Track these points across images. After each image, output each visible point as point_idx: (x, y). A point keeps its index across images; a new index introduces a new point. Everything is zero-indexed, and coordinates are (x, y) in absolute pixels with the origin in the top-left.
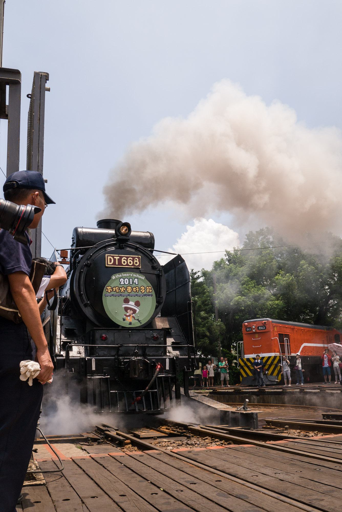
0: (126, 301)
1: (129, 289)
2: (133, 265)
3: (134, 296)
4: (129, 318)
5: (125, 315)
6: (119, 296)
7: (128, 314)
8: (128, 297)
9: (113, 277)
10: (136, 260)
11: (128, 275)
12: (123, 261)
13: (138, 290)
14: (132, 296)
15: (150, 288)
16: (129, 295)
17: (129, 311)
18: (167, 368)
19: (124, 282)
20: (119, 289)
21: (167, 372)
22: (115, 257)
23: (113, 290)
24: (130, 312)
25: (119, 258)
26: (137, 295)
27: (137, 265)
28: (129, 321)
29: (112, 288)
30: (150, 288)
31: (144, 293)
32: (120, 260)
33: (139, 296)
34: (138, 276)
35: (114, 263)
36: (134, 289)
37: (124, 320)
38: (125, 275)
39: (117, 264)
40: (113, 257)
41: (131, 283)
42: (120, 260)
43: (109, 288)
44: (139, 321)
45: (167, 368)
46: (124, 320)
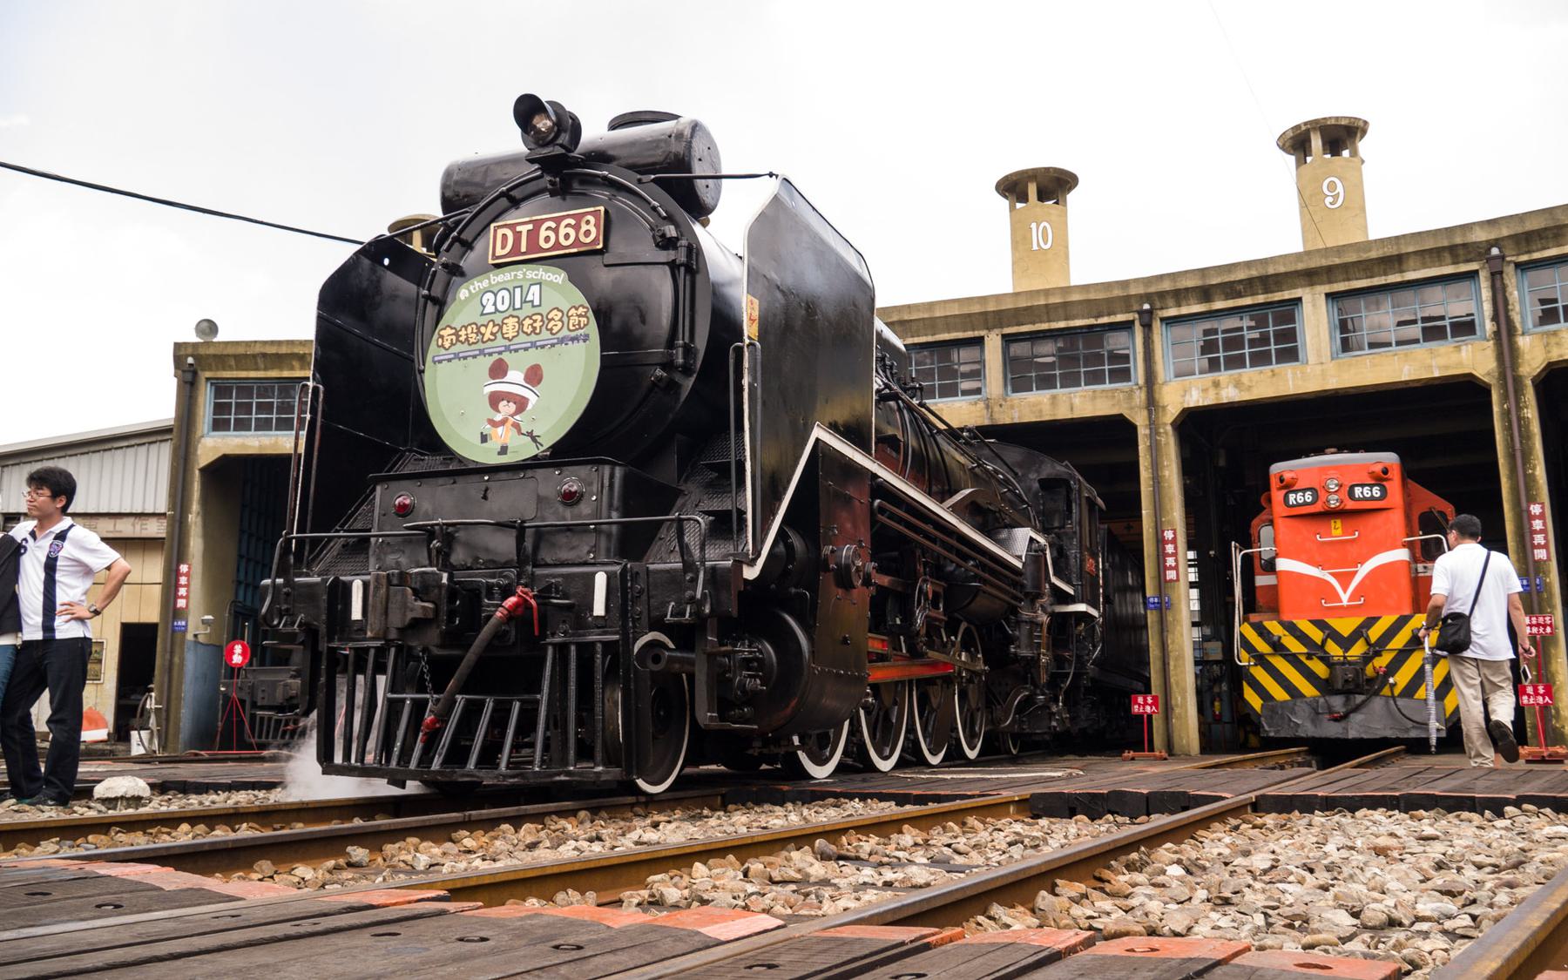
0: (498, 370)
1: (510, 327)
2: (577, 242)
3: (526, 349)
4: (500, 430)
6: (474, 357)
7: (498, 418)
8: (506, 356)
10: (588, 222)
12: (543, 233)
13: (538, 325)
15: (581, 310)
16: (507, 349)
18: (599, 609)
20: (478, 332)
21: (601, 624)
22: (519, 228)
23: (458, 336)
24: (507, 408)
25: (530, 227)
26: (534, 345)
27: (588, 240)
30: (581, 310)
31: (560, 335)
32: (533, 235)
33: (543, 347)
35: (516, 249)
37: (484, 438)
39: (523, 249)
40: (512, 227)
41: (518, 305)
42: (533, 235)
43: (449, 331)
44: (534, 439)
45: (599, 609)
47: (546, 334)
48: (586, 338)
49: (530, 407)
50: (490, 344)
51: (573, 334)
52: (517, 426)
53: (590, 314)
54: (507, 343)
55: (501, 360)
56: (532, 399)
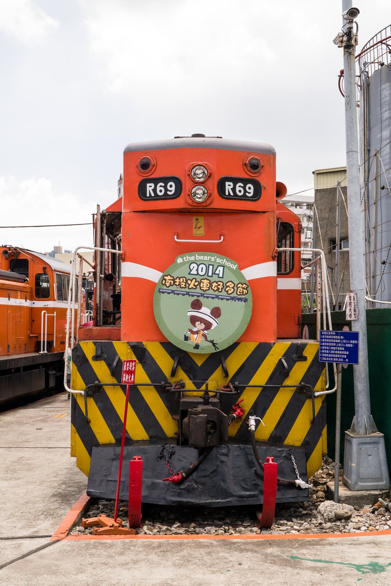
0: (197, 305)
1: (205, 284)
3: (213, 298)
4: (195, 336)
5: (191, 331)
7: (195, 330)
8: (201, 299)
9: (179, 260)
11: (206, 258)
13: (220, 287)
14: (207, 297)
15: (244, 286)
16: (202, 295)
17: (197, 323)
19: (197, 270)
20: (186, 282)
23: (175, 282)
24: (200, 326)
26: (217, 297)
28: (195, 342)
29: (174, 280)
31: (232, 295)
33: (222, 299)
34: (225, 262)
36: (215, 284)
37: (186, 338)
38: (201, 258)
41: (210, 274)
44: (214, 344)
46: (186, 338)
47: (224, 293)
48: (246, 300)
49: (213, 328)
50: (192, 290)
51: (239, 297)
52: (204, 336)
53: (249, 289)
54: (202, 292)
55: (198, 300)
56: (215, 325)
